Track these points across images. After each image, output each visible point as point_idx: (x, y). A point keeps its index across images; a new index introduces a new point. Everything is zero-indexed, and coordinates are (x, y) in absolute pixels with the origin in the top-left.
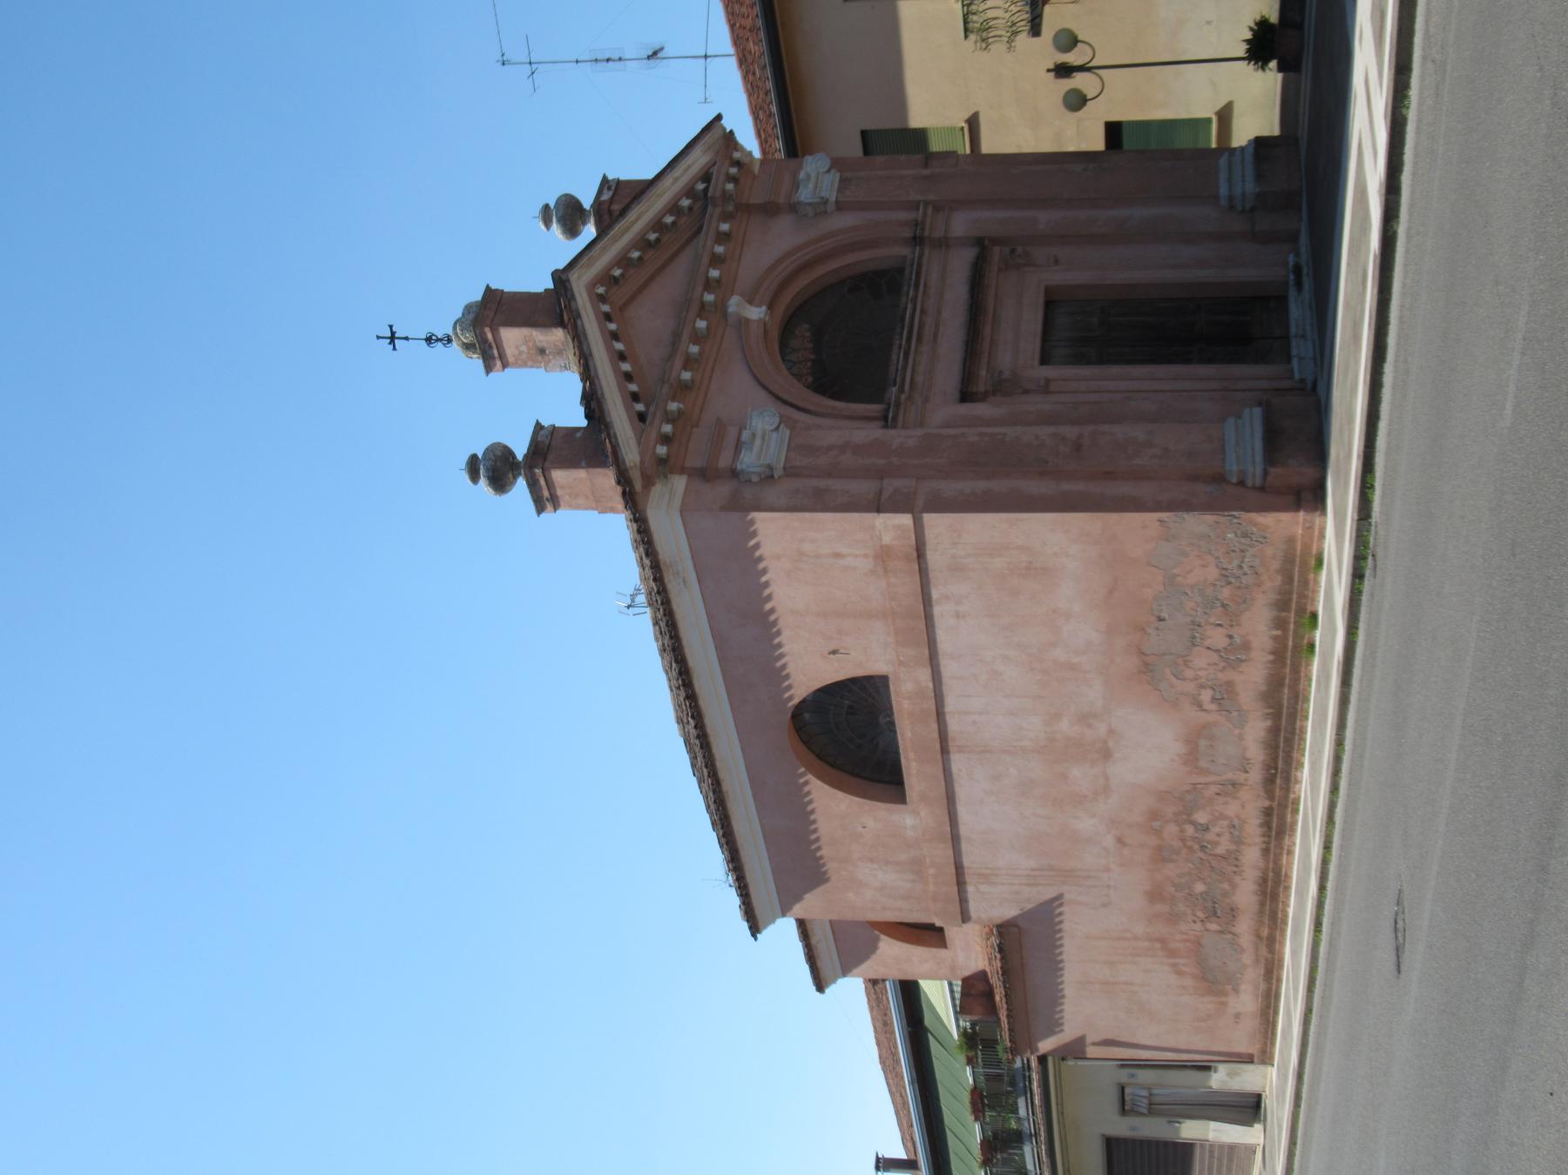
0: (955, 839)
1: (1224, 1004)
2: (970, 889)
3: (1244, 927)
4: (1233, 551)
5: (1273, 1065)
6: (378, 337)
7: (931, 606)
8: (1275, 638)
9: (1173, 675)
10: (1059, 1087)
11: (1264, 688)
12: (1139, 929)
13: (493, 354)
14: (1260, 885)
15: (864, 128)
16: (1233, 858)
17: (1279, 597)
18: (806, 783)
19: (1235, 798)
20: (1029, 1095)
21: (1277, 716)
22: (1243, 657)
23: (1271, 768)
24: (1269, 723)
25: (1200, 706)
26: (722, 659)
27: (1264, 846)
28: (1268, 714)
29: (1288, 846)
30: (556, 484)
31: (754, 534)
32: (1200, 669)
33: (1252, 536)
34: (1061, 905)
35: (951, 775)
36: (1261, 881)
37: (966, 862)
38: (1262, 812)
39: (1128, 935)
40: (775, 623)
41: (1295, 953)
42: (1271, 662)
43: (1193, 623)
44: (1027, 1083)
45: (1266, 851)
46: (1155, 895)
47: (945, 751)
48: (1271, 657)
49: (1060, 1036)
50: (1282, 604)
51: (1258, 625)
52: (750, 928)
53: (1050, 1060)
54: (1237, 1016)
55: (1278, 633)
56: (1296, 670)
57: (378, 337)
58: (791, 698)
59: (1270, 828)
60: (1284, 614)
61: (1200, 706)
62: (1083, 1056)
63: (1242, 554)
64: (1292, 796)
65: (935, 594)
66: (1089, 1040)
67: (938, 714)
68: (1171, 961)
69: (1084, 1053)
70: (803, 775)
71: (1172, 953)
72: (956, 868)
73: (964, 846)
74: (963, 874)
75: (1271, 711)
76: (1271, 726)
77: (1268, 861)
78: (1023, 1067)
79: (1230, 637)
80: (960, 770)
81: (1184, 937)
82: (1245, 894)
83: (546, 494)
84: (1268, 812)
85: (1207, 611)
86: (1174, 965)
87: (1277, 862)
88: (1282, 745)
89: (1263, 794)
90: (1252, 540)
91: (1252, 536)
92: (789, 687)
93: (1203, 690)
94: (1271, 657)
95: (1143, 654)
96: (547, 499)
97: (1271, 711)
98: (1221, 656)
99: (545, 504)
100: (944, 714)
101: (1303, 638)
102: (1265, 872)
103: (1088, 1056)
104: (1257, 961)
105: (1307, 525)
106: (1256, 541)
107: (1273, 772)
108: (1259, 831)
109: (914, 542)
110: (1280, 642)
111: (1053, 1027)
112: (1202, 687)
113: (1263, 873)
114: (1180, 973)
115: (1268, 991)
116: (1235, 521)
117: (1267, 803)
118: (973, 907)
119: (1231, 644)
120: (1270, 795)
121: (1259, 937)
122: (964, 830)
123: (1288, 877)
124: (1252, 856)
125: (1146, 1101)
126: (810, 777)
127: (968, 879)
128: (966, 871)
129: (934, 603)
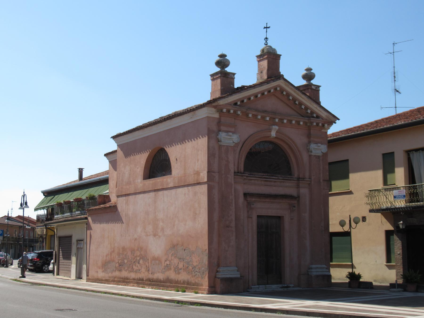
0: (135, 194)
1: (100, 269)
2: (124, 198)
3: (117, 274)
4: (200, 269)
5: (86, 282)
6: (267, 23)
8: (181, 281)
9: (172, 254)
11: (170, 278)
12: (116, 245)
14: (127, 277)
17: (190, 282)
18: (147, 152)
19: (146, 271)
20: (81, 214)
21: (164, 282)
22: (176, 273)
23: (152, 280)
24: (162, 280)
25: (166, 261)
27: (135, 279)
28: (164, 279)
30: (217, 80)
32: (174, 261)
34: (121, 223)
36: (127, 278)
37: (130, 197)
40: (183, 143)
41: (107, 287)
42: (175, 280)
43: (184, 259)
44: (83, 214)
45: (134, 279)
46: (124, 249)
47: (155, 191)
48: (177, 280)
50: (188, 283)
51: (183, 277)
52: (113, 136)
53: (86, 220)
54: (97, 272)
55: (182, 282)
56: (173, 287)
57: (267, 23)
58: (166, 147)
59: (139, 280)
61: (166, 261)
63: (199, 272)
64: (146, 286)
65: (189, 188)
66: (91, 231)
67: (163, 189)
68: (109, 254)
69: (88, 230)
70: (149, 151)
71: (111, 254)
72: (129, 194)
73: (134, 196)
74: (128, 196)
75: (165, 280)
76: (161, 280)
77: (132, 280)
79: (181, 269)
81: (115, 257)
82: (124, 274)
83: (215, 77)
84: (142, 280)
85: (187, 263)
86: (108, 255)
89: (147, 278)
93: (169, 261)
94: (177, 280)
96: (213, 78)
97: (165, 280)
98: (177, 267)
100: (163, 190)
102: (130, 279)
103: (87, 231)
104: (110, 277)
105: (205, 289)
108: (138, 277)
111: (94, 221)
112: (170, 261)
113: (129, 278)
114: (107, 256)
116: (206, 270)
117: (144, 279)
118: (120, 199)
120: (146, 280)
121: (115, 278)
122: (137, 196)
123: (128, 285)
124: (133, 275)
125: (80, 247)
126: (149, 153)
127: (127, 197)
128: (128, 197)
129: (188, 187)
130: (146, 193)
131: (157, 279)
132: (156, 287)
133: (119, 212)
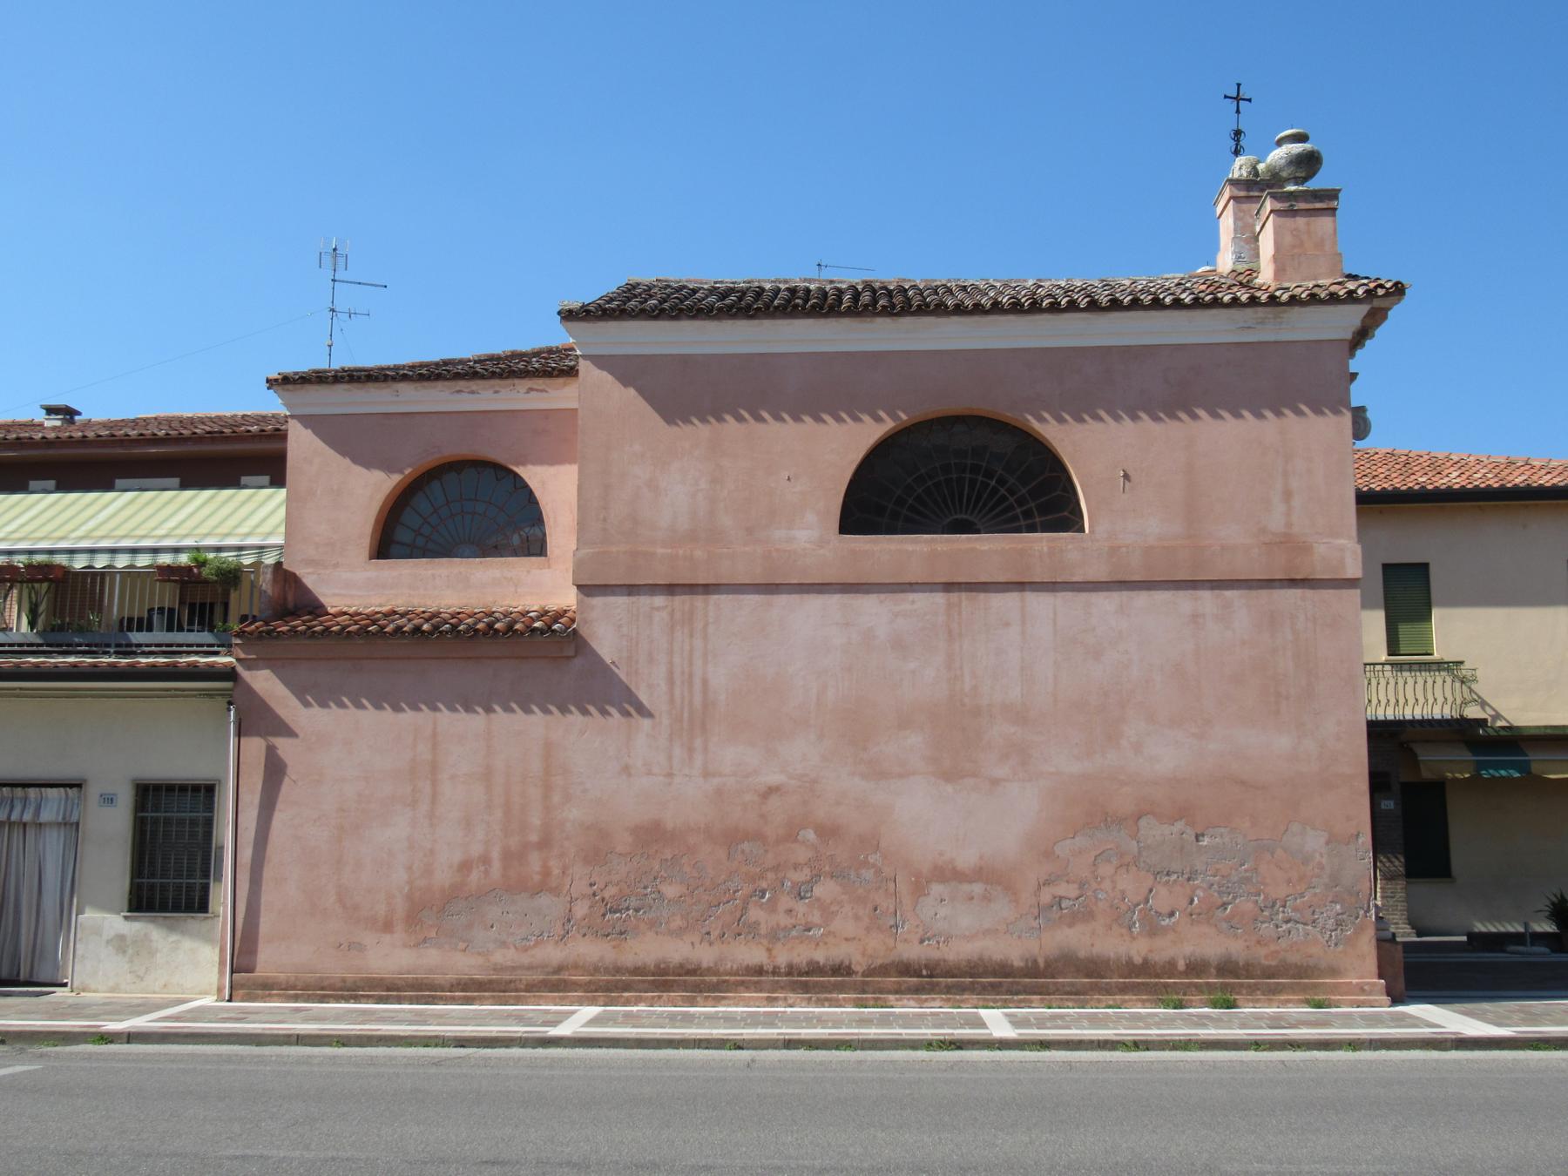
3: (590, 950)
4: (1314, 912)
7: (1212, 588)
9: (1104, 852)
10: (116, 694)
12: (574, 814)
13: (1252, 191)
15: (1433, 570)
16: (743, 929)
19: (868, 929)
20: (45, 648)
22: (1137, 929)
24: (1018, 963)
26: (1127, 349)
29: (785, 999)
30: (1313, 218)
31: (1318, 411)
32: (1113, 882)
33: (1339, 931)
35: (903, 591)
38: (842, 963)
39: (556, 798)
40: (1173, 416)
44: (83, 648)
46: (652, 835)
47: (949, 587)
49: (294, 701)
50: (1227, 968)
51: (1211, 944)
52: (570, 311)
53: (228, 685)
54: (356, 947)
58: (1041, 420)
60: (1213, 971)
62: (242, 734)
63: (1310, 922)
64: (891, 997)
66: (283, 745)
68: (495, 854)
69: (249, 734)
76: (1012, 966)
78: (130, 645)
79: (1172, 914)
80: (913, 602)
82: (648, 949)
83: (1302, 206)
84: (842, 969)
86: (485, 860)
87: (736, 986)
90: (1332, 931)
91: (1339, 931)
92: (1061, 420)
93: (1076, 886)
95: (1139, 818)
96: (1292, 206)
98: (1138, 905)
99: (1287, 202)
100: (1023, 590)
101: (1238, 994)
103: (242, 739)
104: (497, 969)
106: (1331, 936)
107: (924, 972)
109: (1318, 577)
110: (1170, 968)
111: (309, 692)
112: (1082, 885)
114: (465, 866)
115: (432, 987)
116: (1362, 912)
118: (598, 601)
119: (1159, 914)
121: (559, 969)
122: (782, 600)
123: (717, 1001)
124: (753, 954)
129: (1217, 592)
130: (867, 592)
131: (969, 961)
132: (985, 1000)
133: (608, 661)
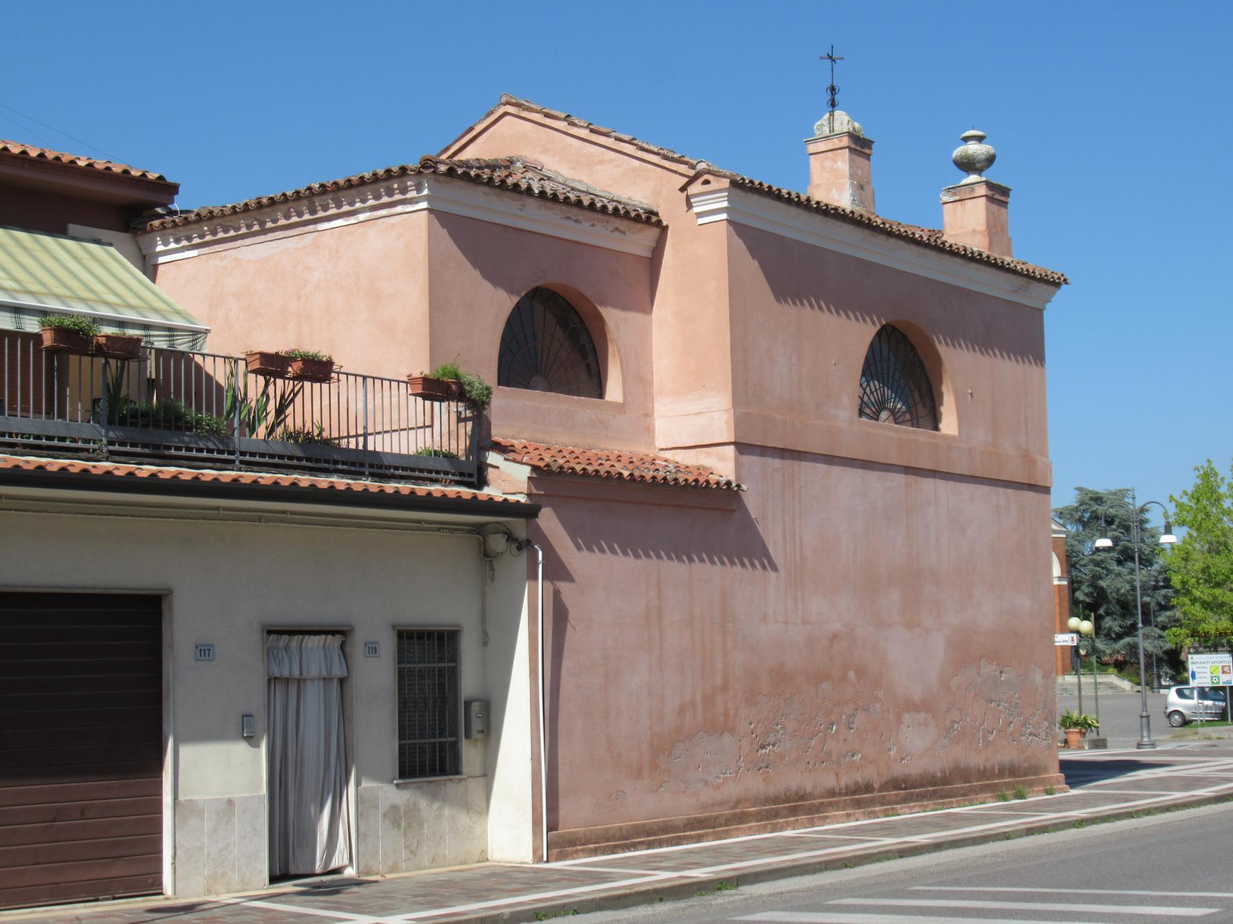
0: (830, 459)
1: (639, 775)
2: (777, 463)
5: (533, 863)
6: (832, 47)
8: (993, 768)
14: (797, 793)
17: (1016, 766)
18: (874, 323)
21: (945, 781)
23: (905, 783)
24: (939, 775)
25: (949, 710)
27: (837, 790)
28: (945, 773)
34: (764, 567)
35: (887, 471)
36: (802, 793)
37: (806, 465)
42: (979, 769)
43: (1000, 701)
45: (832, 793)
48: (982, 768)
55: (997, 771)
56: (983, 789)
57: (832, 47)
58: (940, 342)
59: (854, 793)
60: (1007, 773)
61: (949, 710)
65: (1010, 491)
67: (934, 471)
68: (698, 699)
70: (880, 322)
71: (708, 699)
72: (800, 452)
73: (821, 467)
74: (793, 458)
75: (948, 774)
77: (823, 797)
81: (732, 713)
84: (868, 788)
85: (1007, 711)
86: (693, 703)
88: (917, 790)
89: (885, 779)
94: (982, 768)
97: (948, 774)
102: (811, 796)
104: (704, 807)
105: (1059, 779)
107: (903, 786)
108: (850, 782)
111: (585, 537)
113: (810, 794)
114: (681, 711)
117: (876, 786)
120: (884, 787)
121: (737, 803)
122: (836, 470)
125: (296, 673)
126: (878, 327)
127: (788, 462)
128: (796, 463)
130: (873, 469)
131: (920, 775)
132: (935, 804)
133: (754, 517)
